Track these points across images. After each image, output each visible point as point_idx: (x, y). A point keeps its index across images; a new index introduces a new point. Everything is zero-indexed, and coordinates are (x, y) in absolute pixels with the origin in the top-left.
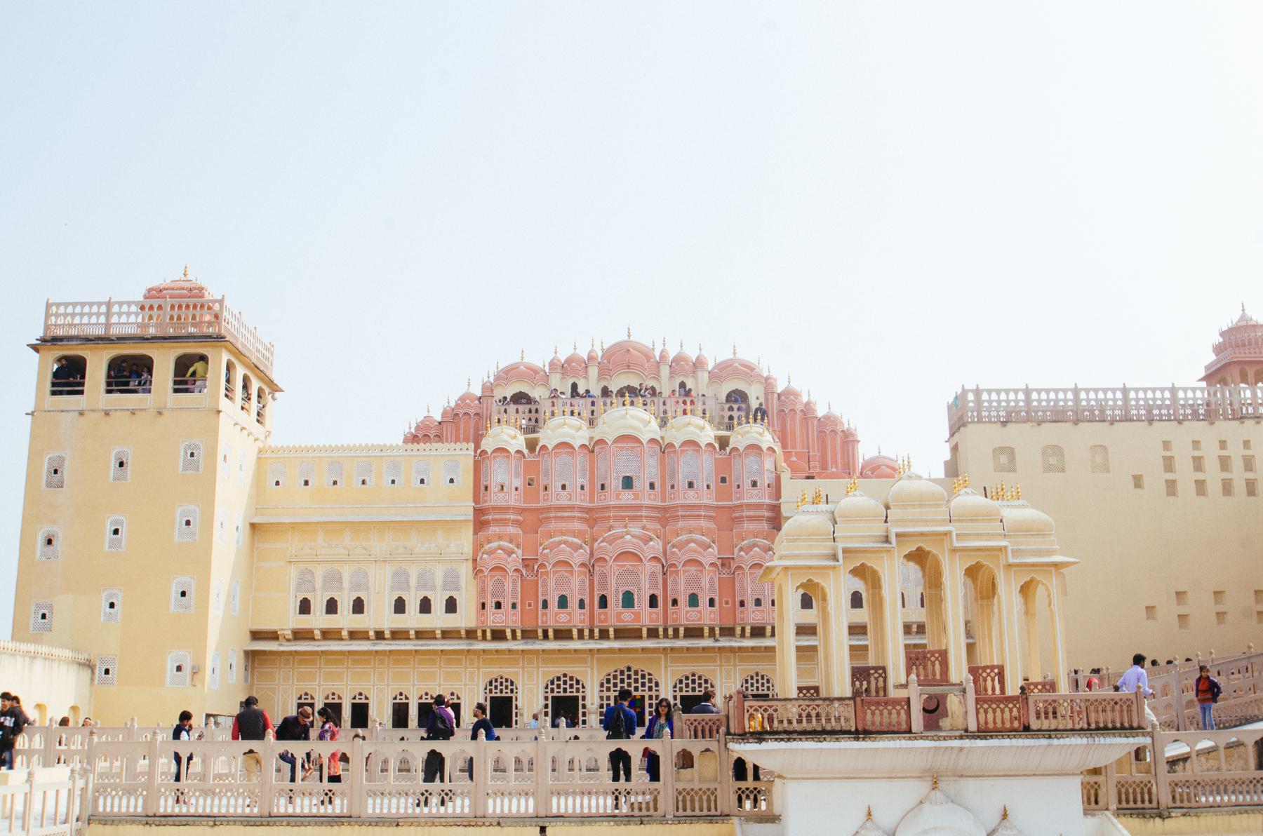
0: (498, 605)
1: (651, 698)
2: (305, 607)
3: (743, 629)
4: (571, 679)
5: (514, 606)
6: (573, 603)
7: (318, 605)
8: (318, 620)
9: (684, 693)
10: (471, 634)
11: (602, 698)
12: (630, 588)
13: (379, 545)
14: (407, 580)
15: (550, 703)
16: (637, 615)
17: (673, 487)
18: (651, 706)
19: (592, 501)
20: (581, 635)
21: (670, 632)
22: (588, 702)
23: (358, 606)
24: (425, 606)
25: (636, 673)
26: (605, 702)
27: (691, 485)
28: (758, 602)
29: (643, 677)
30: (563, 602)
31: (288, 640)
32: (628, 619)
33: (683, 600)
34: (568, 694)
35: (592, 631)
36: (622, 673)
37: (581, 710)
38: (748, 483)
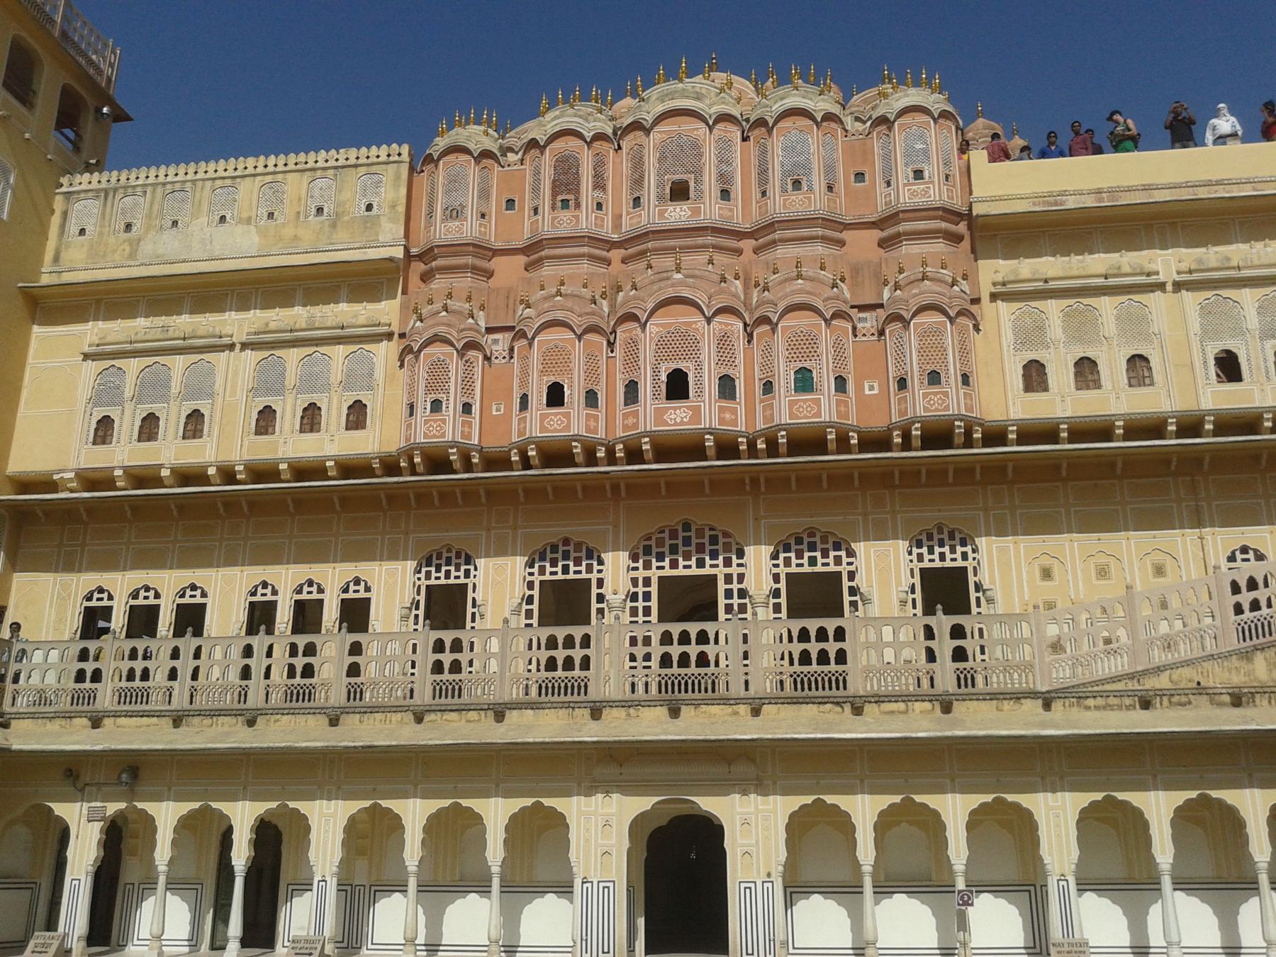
0: (436, 406)
1: (728, 578)
2: (104, 431)
3: (906, 436)
4: (578, 547)
5: (467, 408)
6: (574, 394)
7: (127, 422)
8: (124, 453)
9: (793, 569)
10: (390, 466)
11: (635, 582)
12: (682, 365)
13: (237, 323)
14: (283, 375)
15: (536, 593)
16: (696, 411)
17: (764, 193)
18: (729, 594)
19: (617, 226)
20: (591, 459)
21: (761, 445)
22: (607, 590)
23: (194, 424)
24: (311, 418)
25: (700, 533)
26: (641, 589)
27: (797, 184)
28: (934, 378)
29: (714, 540)
30: (555, 396)
31: (72, 491)
32: (678, 418)
33: (785, 378)
34: (571, 576)
35: (611, 452)
36: (673, 534)
37: (594, 606)
38: (903, 173)
